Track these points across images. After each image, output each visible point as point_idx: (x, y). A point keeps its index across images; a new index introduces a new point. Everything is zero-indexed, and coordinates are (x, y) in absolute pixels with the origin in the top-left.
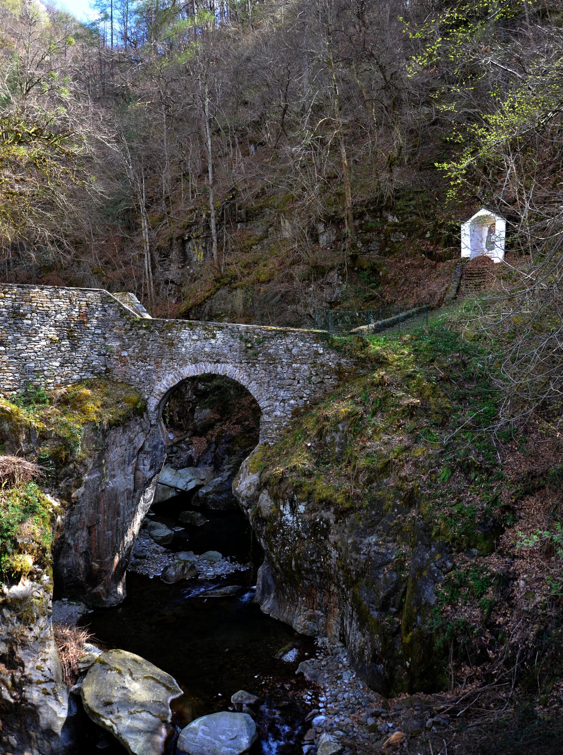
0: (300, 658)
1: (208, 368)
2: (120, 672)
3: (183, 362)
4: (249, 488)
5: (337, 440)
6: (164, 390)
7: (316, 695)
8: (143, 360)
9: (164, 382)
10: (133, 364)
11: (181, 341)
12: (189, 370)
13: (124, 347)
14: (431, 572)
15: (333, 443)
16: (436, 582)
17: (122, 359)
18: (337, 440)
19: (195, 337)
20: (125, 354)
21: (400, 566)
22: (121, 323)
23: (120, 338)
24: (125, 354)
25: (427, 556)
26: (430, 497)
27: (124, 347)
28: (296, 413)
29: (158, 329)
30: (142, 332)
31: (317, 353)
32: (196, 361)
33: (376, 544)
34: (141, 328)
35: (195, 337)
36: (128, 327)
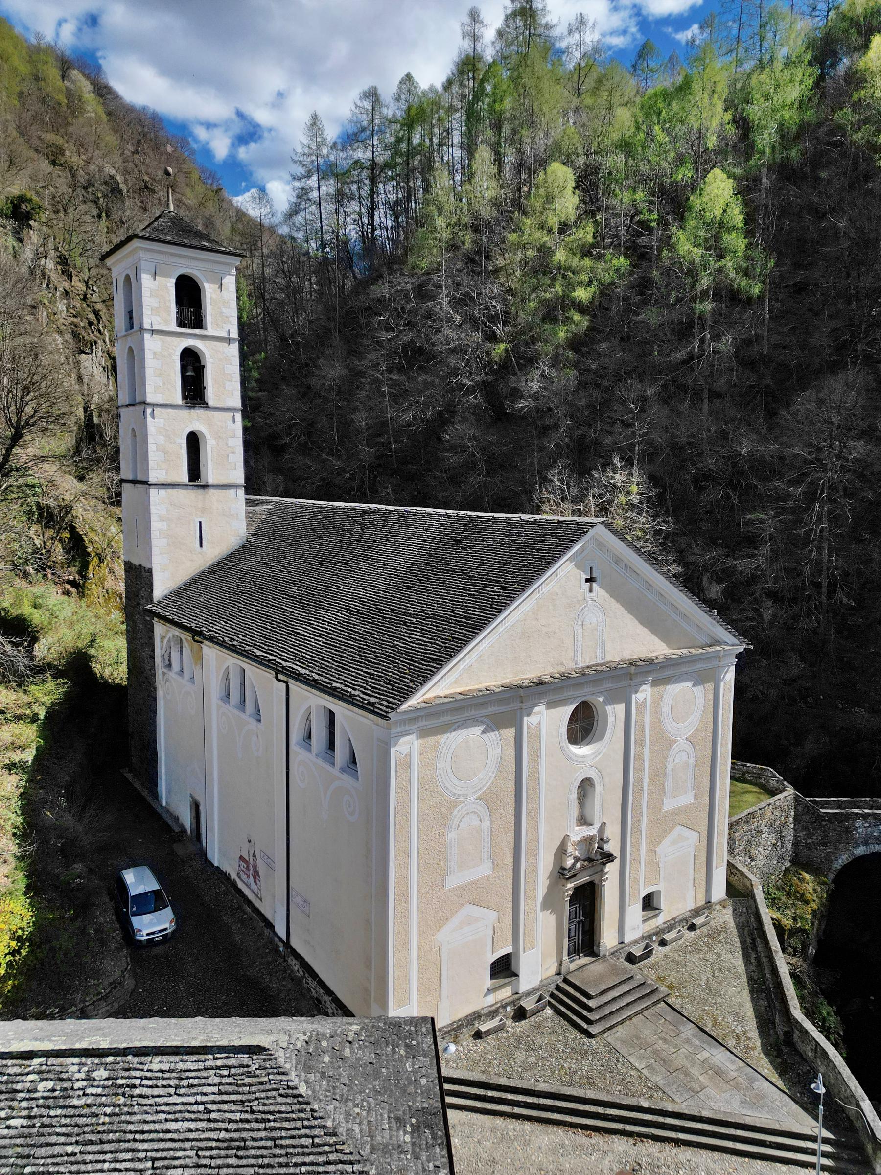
3: (857, 846)
6: (839, 867)
8: (824, 844)
9: (840, 861)
10: (817, 849)
11: (856, 829)
12: (860, 851)
13: (810, 835)
17: (808, 846)
19: (867, 825)
20: (810, 841)
22: (808, 817)
23: (806, 829)
24: (810, 841)
27: (810, 835)
29: (837, 819)
30: (824, 823)
32: (866, 843)
34: (825, 820)
35: (867, 825)
36: (813, 820)
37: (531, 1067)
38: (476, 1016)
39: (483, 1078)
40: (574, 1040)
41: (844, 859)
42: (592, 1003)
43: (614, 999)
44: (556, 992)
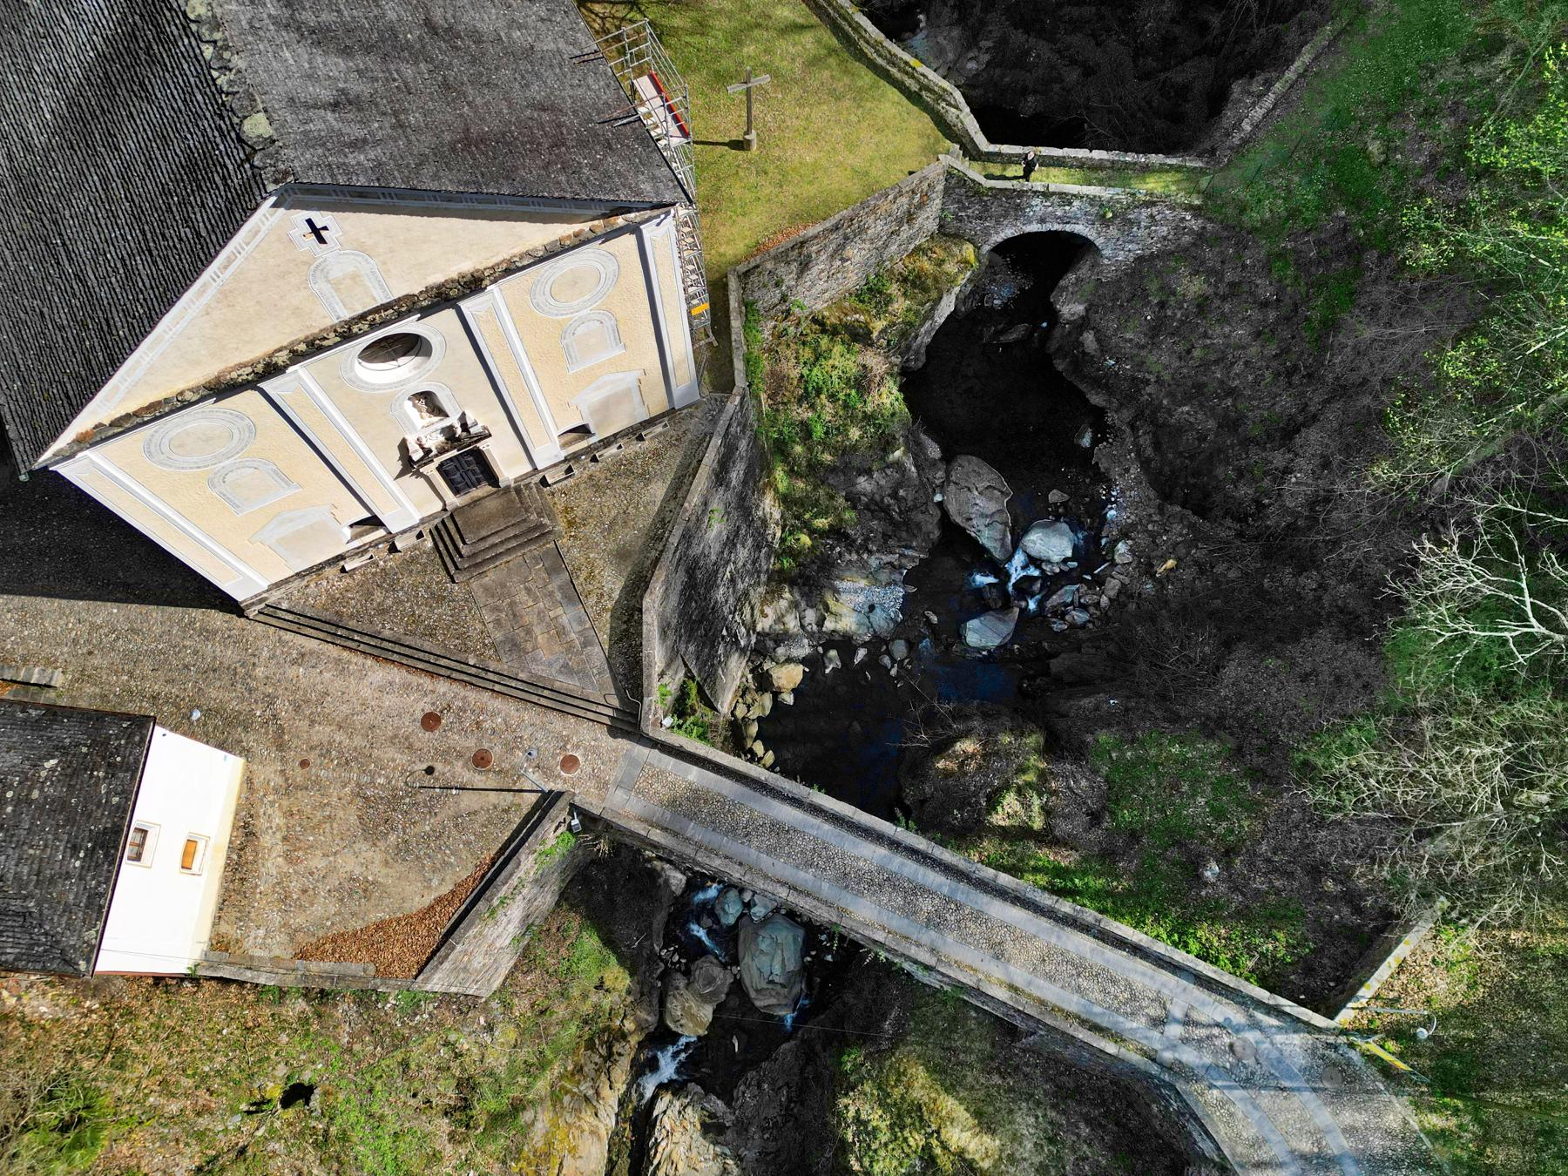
0: (1095, 442)
1: (1057, 227)
2: (969, 489)
4: (1073, 315)
5: (1179, 316)
7: (1109, 489)
12: (1034, 227)
14: (1228, 457)
15: (1173, 317)
16: (1228, 464)
18: (1179, 316)
21: (1202, 438)
25: (1229, 442)
26: (1251, 398)
28: (1139, 259)
31: (1183, 219)
33: (1188, 413)
37: (383, 611)
38: (341, 557)
39: (335, 619)
40: (437, 583)
41: (1008, 232)
42: (464, 550)
43: (494, 546)
44: (440, 526)
